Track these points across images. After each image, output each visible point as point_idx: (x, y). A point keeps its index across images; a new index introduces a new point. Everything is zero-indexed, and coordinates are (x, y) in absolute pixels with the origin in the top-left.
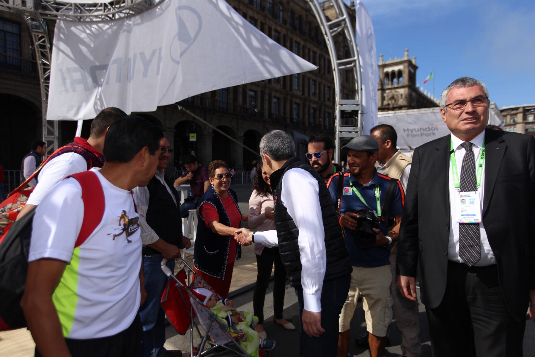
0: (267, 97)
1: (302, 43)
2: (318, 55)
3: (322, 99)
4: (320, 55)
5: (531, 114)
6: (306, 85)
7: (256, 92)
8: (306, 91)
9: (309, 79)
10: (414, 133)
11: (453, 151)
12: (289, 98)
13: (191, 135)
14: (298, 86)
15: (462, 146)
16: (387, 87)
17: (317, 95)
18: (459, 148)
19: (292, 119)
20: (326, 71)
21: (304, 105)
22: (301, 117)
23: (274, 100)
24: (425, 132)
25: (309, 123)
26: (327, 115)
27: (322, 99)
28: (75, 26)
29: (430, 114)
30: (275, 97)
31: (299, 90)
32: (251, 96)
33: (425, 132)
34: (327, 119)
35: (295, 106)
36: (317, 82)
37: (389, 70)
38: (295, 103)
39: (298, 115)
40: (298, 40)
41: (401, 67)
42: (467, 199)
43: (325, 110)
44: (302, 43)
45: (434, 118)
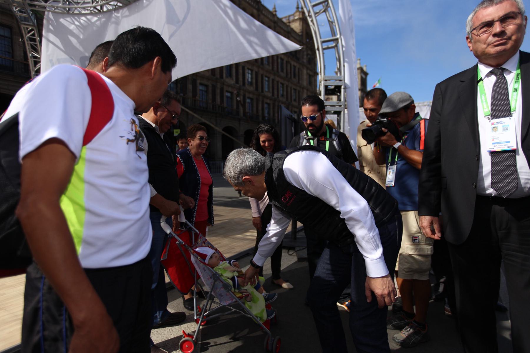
3: (289, 99)
4: (286, 62)
6: (276, 87)
7: (232, 93)
8: (276, 93)
9: (278, 82)
11: (481, 79)
13: (175, 131)
14: (269, 88)
15: (491, 73)
17: (285, 96)
18: (488, 75)
19: (264, 117)
20: (292, 76)
22: (272, 115)
23: (248, 100)
27: (289, 99)
28: (63, 18)
30: (249, 98)
31: (269, 91)
32: (227, 97)
35: (266, 106)
36: (285, 85)
38: (267, 103)
39: (269, 113)
42: (500, 127)
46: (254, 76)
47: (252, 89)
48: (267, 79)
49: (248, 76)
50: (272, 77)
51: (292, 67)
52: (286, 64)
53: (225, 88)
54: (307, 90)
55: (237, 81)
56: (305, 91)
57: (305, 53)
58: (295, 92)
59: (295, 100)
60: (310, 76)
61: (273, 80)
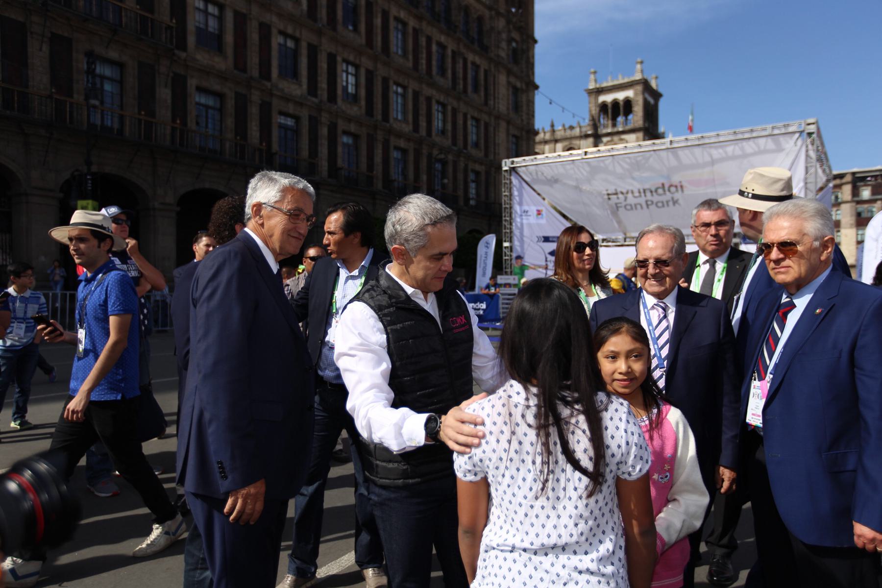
0: (324, 131)
1: (412, 23)
2: (449, 52)
3: (460, 143)
4: (453, 52)
5: (865, 185)
7: (297, 119)
8: (423, 124)
9: (429, 99)
10: (631, 200)
12: (380, 136)
14: (405, 113)
16: (605, 131)
17: (450, 134)
20: (470, 89)
24: (656, 198)
26: (472, 176)
27: (460, 143)
29: (663, 154)
30: (345, 133)
31: (405, 120)
33: (656, 198)
34: (473, 186)
35: (395, 154)
36: (449, 108)
37: (608, 98)
38: (397, 148)
39: (404, 174)
40: (402, 15)
41: (629, 93)
43: (466, 166)
44: (412, 23)
45: (673, 162)
46: (363, 80)
47: (354, 111)
48: (400, 90)
49: (348, 80)
50: (413, 85)
51: (469, 65)
52: (454, 58)
53: (276, 104)
54: (509, 123)
56: (503, 125)
57: (504, 36)
58: (478, 127)
59: (476, 145)
60: (516, 90)
61: (416, 95)
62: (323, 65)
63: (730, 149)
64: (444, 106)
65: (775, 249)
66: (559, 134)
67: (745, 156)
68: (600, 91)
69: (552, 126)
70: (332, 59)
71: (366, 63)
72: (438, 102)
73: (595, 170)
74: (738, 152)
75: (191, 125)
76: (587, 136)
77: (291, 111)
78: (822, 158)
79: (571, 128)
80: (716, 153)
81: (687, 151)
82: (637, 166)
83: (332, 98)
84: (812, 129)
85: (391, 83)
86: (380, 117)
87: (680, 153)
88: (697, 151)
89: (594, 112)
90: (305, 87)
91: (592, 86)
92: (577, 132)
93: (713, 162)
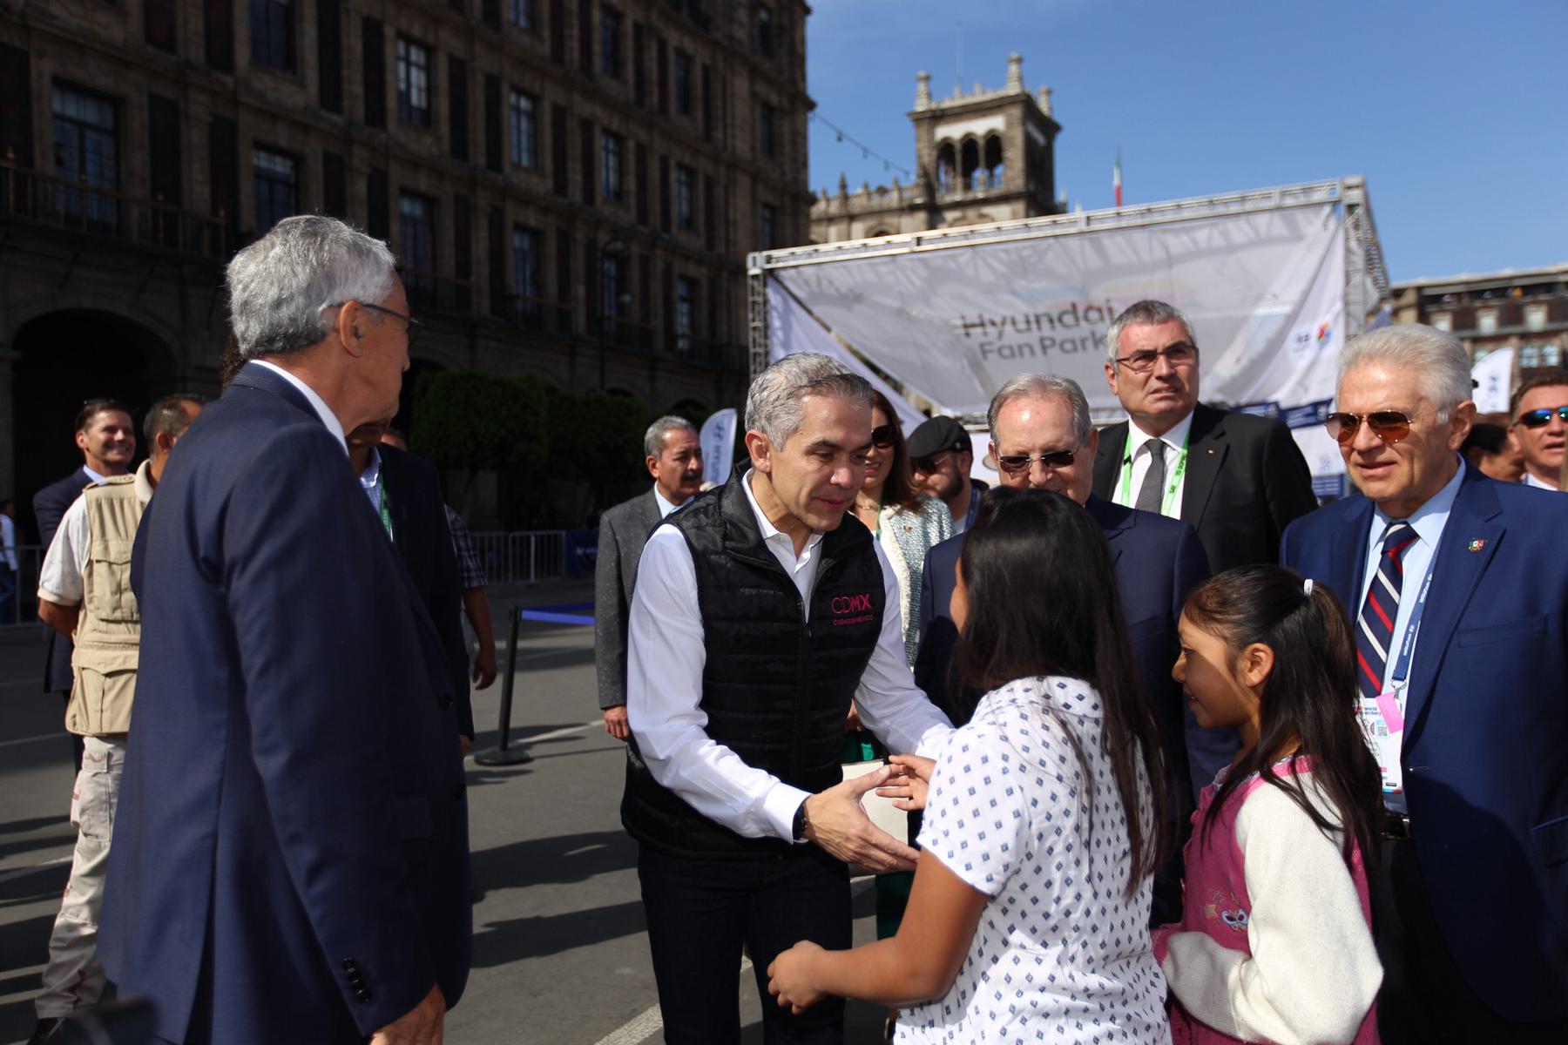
3: (655, 218)
4: (638, 28)
5: (1443, 311)
7: (297, 159)
8: (575, 176)
9: (587, 125)
10: (1011, 336)
12: (483, 200)
14: (535, 151)
17: (633, 200)
19: (501, 298)
21: (565, 237)
22: (552, 288)
24: (1060, 333)
25: (595, 319)
26: (680, 289)
27: (655, 218)
29: (1073, 243)
30: (407, 192)
31: (537, 168)
33: (1060, 333)
35: (518, 241)
36: (631, 144)
37: (954, 131)
38: (521, 228)
41: (997, 122)
45: (1094, 261)
48: (524, 103)
49: (410, 78)
50: (552, 95)
51: (672, 56)
53: (249, 126)
54: (755, 178)
55: (331, 93)
56: (744, 181)
58: (691, 186)
59: (689, 224)
60: (769, 111)
61: (560, 114)
62: (353, 42)
63: (1202, 235)
64: (619, 139)
65: (1364, 426)
66: (857, 204)
67: (1231, 248)
68: (938, 117)
69: (843, 186)
70: (373, 31)
71: (451, 43)
72: (607, 132)
73: (937, 275)
74: (1218, 241)
75: (45, 164)
76: (913, 208)
77: (283, 142)
78: (1374, 258)
79: (882, 191)
80: (1177, 243)
81: (1119, 238)
82: (1022, 267)
83: (376, 115)
84: (1355, 196)
85: (505, 87)
86: (482, 161)
87: (1107, 241)
88: (1140, 237)
89: (926, 160)
90: (313, 88)
91: (921, 106)
92: (893, 199)
93: (1171, 261)
